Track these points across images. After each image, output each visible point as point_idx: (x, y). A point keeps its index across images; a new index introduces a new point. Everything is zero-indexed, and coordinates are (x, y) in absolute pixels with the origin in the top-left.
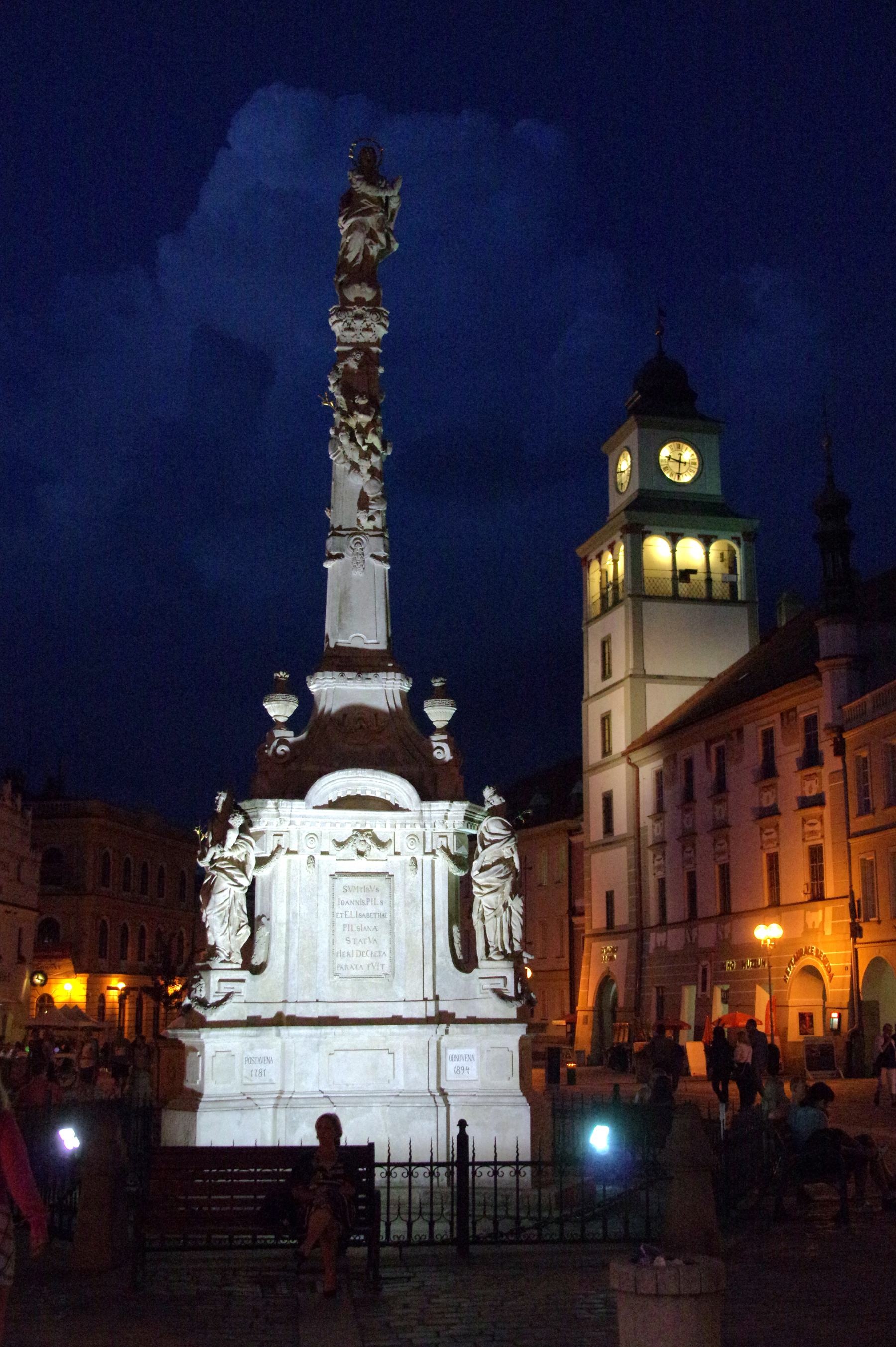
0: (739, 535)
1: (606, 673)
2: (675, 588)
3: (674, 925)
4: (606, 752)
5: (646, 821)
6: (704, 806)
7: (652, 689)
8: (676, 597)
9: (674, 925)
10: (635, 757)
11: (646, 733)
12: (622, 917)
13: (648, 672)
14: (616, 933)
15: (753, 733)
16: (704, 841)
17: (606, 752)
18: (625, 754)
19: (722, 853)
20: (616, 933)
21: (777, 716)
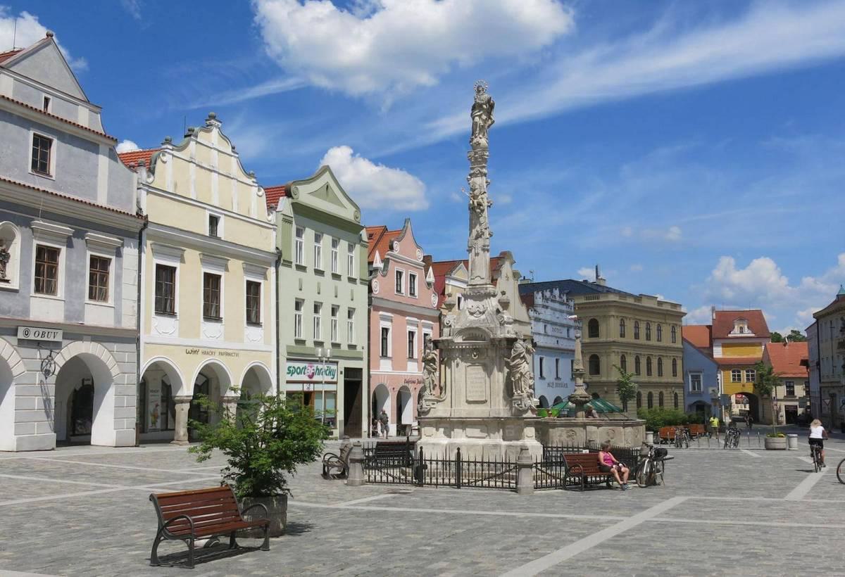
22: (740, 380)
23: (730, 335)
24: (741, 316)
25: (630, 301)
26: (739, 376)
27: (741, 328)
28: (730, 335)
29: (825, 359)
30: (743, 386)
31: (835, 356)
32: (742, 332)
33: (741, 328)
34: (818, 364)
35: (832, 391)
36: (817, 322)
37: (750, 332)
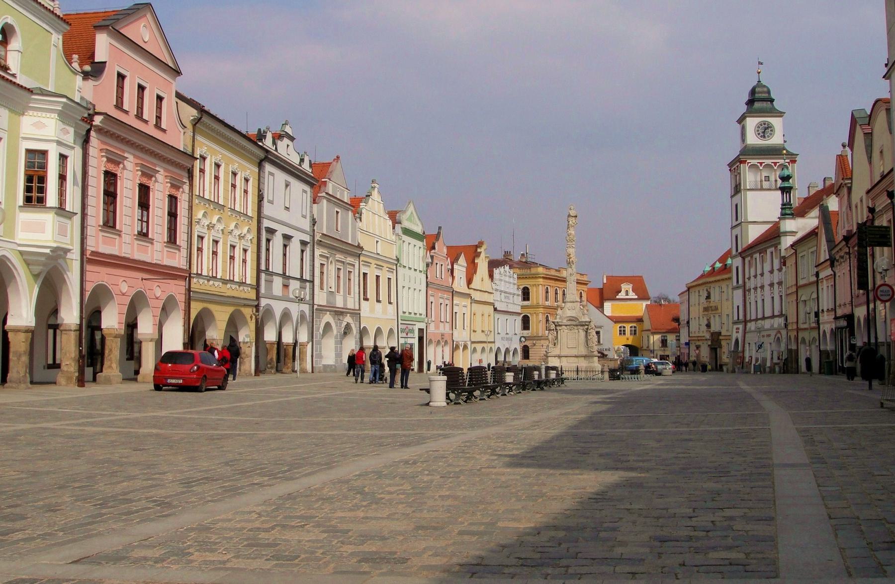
0: (788, 161)
1: (737, 219)
2: (762, 186)
3: (753, 320)
4: (737, 250)
5: (747, 280)
6: (759, 276)
7: (751, 227)
8: (762, 189)
9: (753, 320)
10: (744, 255)
11: (749, 245)
12: (741, 317)
13: (749, 220)
14: (740, 322)
15: (769, 251)
16: (759, 290)
17: (737, 250)
18: (740, 253)
19: (762, 295)
20: (740, 322)
21: (773, 248)
22: (624, 334)
23: (617, 297)
24: (627, 279)
25: (553, 273)
26: (624, 331)
27: (627, 292)
28: (617, 297)
29: (693, 319)
30: (628, 339)
31: (701, 318)
32: (627, 294)
33: (627, 292)
34: (688, 322)
35: (698, 343)
36: (689, 289)
37: (634, 294)
